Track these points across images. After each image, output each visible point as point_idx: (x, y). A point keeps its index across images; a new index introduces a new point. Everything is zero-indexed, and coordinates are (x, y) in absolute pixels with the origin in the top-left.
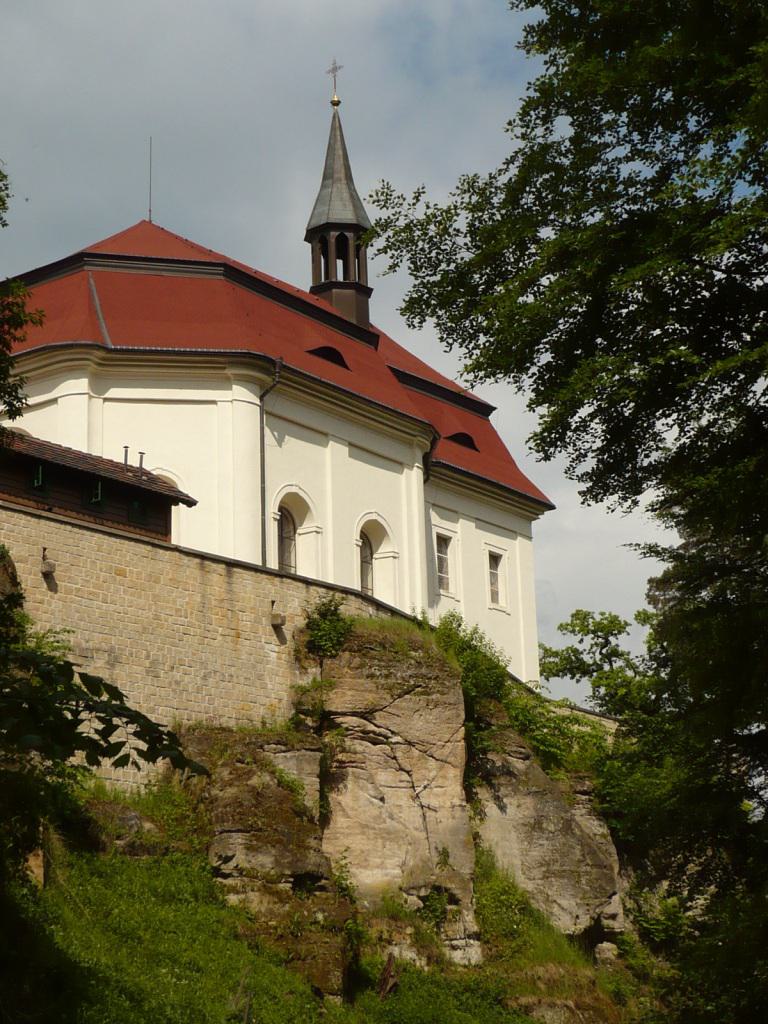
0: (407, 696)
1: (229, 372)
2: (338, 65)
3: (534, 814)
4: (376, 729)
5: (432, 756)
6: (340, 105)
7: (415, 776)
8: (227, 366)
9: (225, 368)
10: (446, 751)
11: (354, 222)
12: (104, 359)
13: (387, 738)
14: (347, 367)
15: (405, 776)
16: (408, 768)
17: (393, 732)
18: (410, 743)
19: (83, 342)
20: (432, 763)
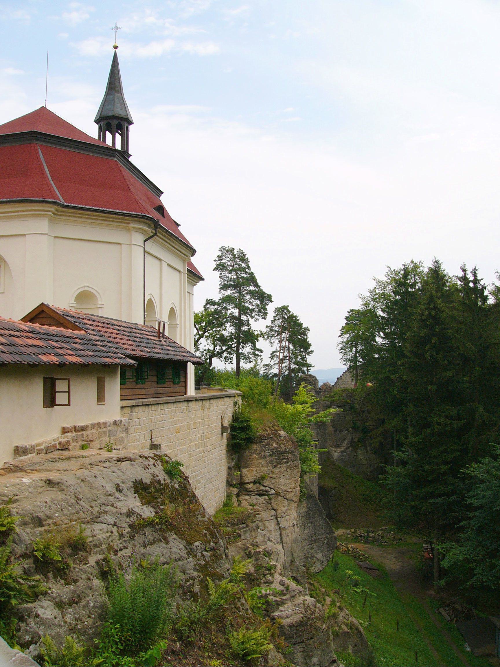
0: (279, 466)
1: (132, 225)
2: (118, 26)
3: (306, 510)
4: (264, 488)
5: (286, 499)
6: (118, 49)
7: (279, 511)
8: (131, 222)
9: (129, 223)
10: (292, 494)
11: (127, 117)
12: (57, 211)
13: (267, 492)
14: (164, 217)
15: (274, 513)
16: (276, 507)
17: (271, 488)
18: (277, 494)
19: (50, 200)
20: (286, 502)
